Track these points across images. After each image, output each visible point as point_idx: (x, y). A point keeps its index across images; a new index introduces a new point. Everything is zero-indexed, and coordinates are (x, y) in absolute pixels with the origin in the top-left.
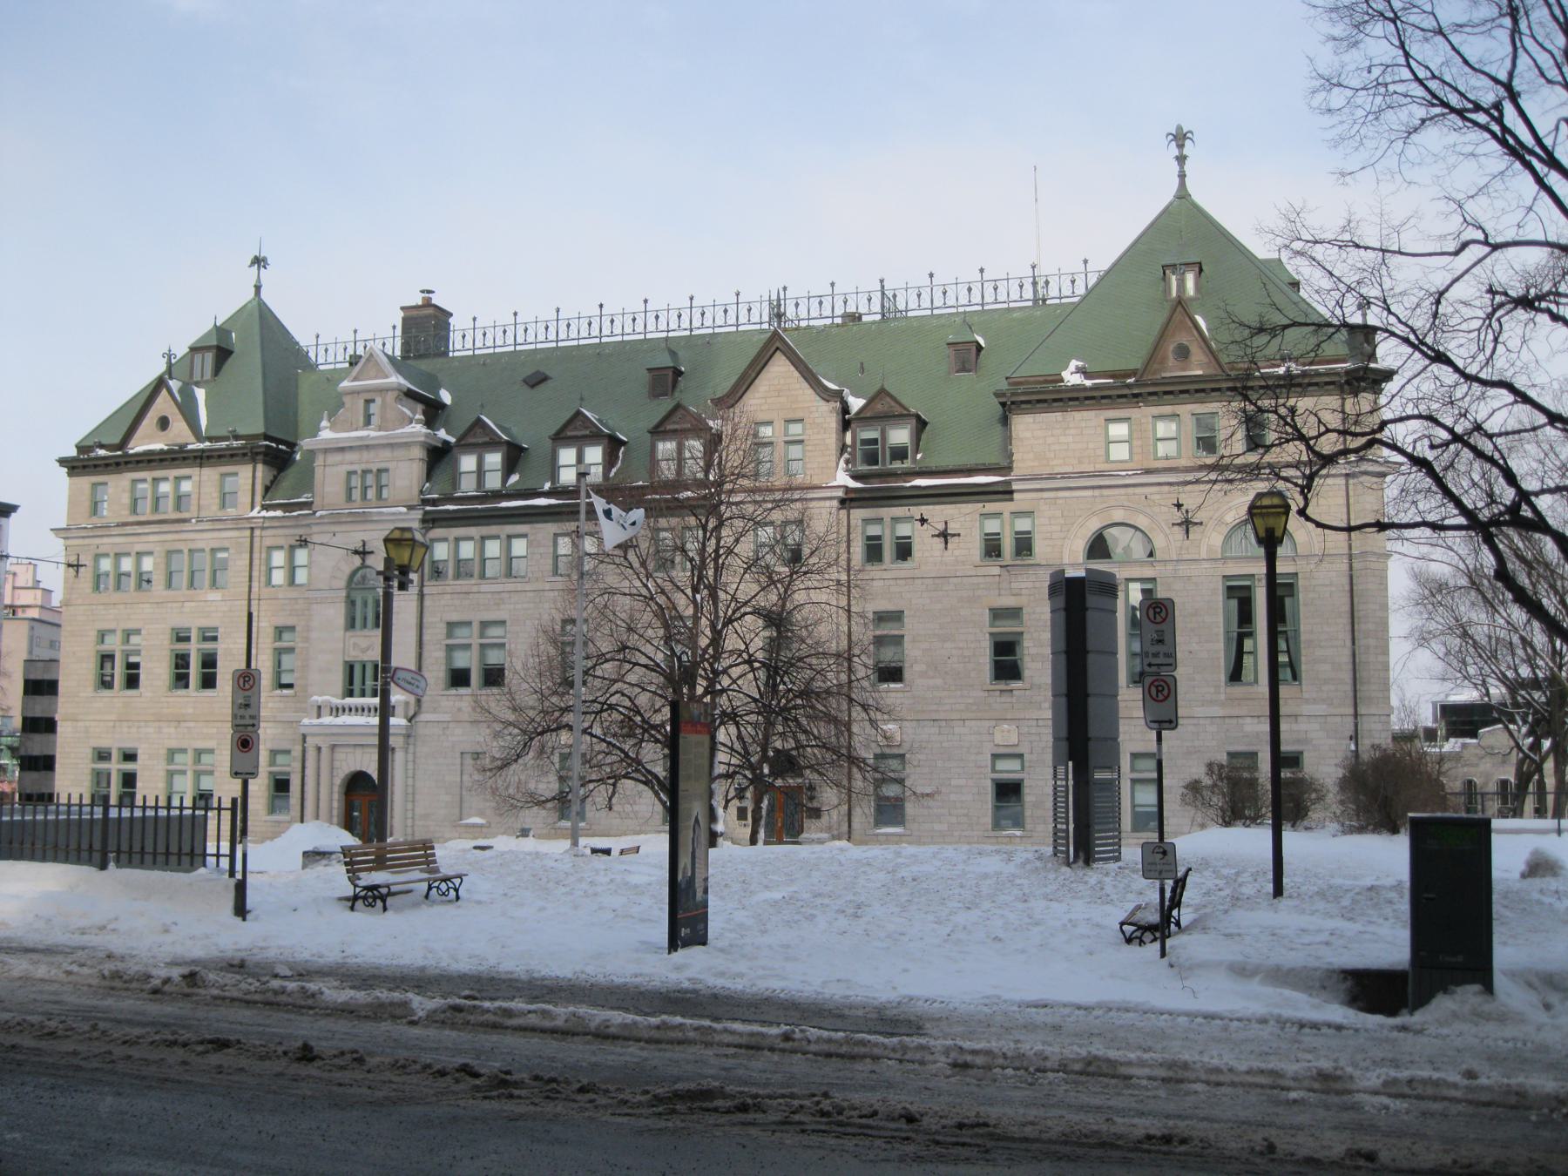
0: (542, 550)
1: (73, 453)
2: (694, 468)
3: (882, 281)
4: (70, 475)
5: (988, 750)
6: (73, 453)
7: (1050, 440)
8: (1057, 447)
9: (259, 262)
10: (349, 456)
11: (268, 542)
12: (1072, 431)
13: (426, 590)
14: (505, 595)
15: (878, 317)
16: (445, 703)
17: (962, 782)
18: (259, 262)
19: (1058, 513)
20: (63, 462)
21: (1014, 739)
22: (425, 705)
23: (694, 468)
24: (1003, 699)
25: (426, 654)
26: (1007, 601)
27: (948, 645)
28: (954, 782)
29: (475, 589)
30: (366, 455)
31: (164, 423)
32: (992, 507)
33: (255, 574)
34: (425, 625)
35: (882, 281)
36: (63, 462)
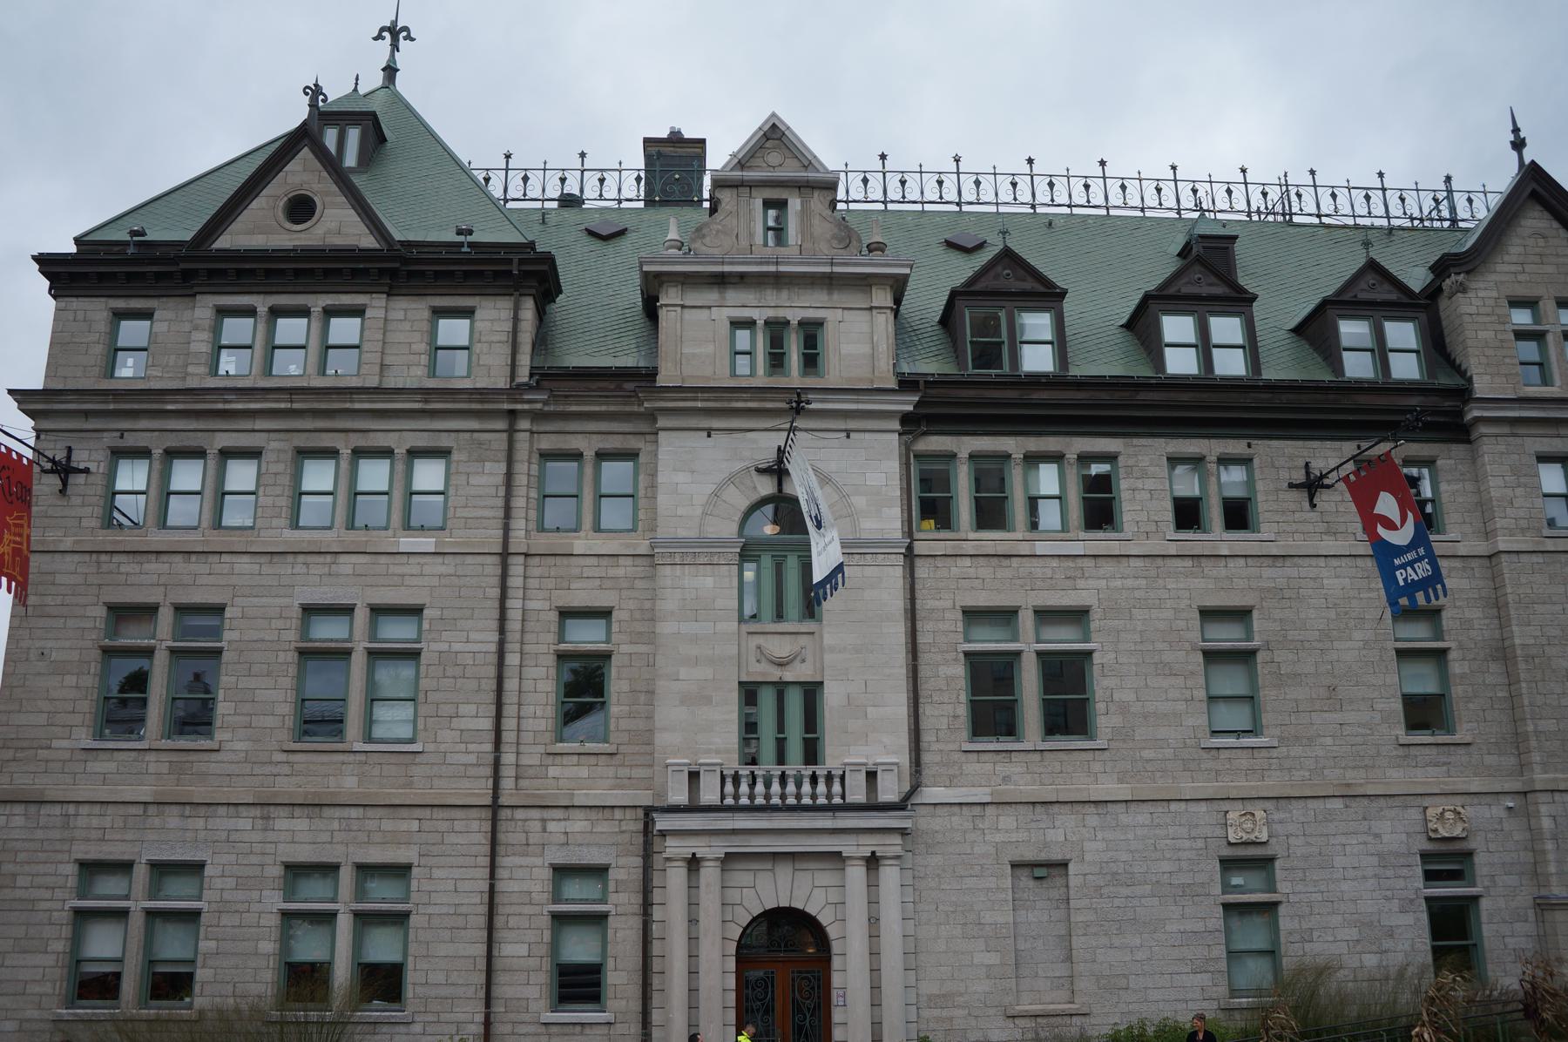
0: (1150, 484)
1: (73, 249)
2: (1406, 368)
3: (1448, 179)
4: (57, 291)
6: (73, 249)
9: (395, 33)
10: (733, 296)
11: (546, 443)
13: (919, 548)
14: (1089, 563)
15: (1446, 224)
16: (972, 767)
18: (395, 33)
20: (47, 263)
22: (927, 772)
23: (1406, 368)
25: (924, 671)
29: (1024, 548)
30: (771, 296)
31: (301, 209)
33: (519, 502)
34: (920, 614)
35: (1448, 179)
36: (47, 263)
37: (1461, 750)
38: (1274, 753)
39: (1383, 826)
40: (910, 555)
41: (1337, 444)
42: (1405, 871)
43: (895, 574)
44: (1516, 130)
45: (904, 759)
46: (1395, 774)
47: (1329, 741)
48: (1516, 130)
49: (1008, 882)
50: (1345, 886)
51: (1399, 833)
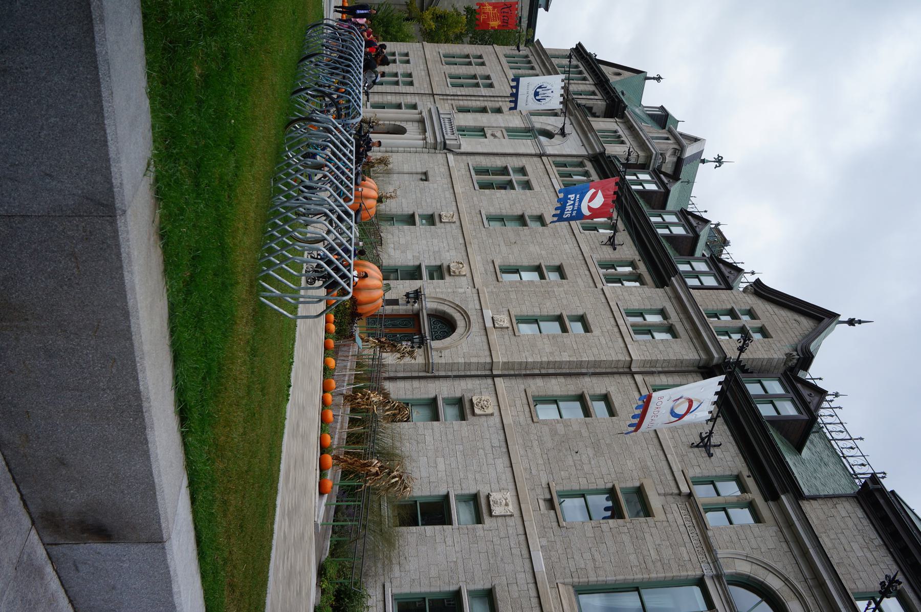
5: (484, 491)
7: (847, 532)
8: (843, 540)
12: (869, 555)
17: (441, 467)
19: (771, 546)
21: (497, 510)
22: (459, 157)
24: (542, 503)
26: (655, 502)
27: (590, 452)
28: (440, 460)
31: (619, 74)
32: (751, 483)
37: (494, 278)
38: (482, 227)
39: (453, 253)
40: (540, 156)
41: (637, 253)
42: (432, 258)
43: (533, 152)
44: (860, 322)
45: (463, 150)
46: (479, 258)
47: (490, 241)
48: (860, 322)
49: (420, 170)
50: (424, 242)
51: (450, 256)
